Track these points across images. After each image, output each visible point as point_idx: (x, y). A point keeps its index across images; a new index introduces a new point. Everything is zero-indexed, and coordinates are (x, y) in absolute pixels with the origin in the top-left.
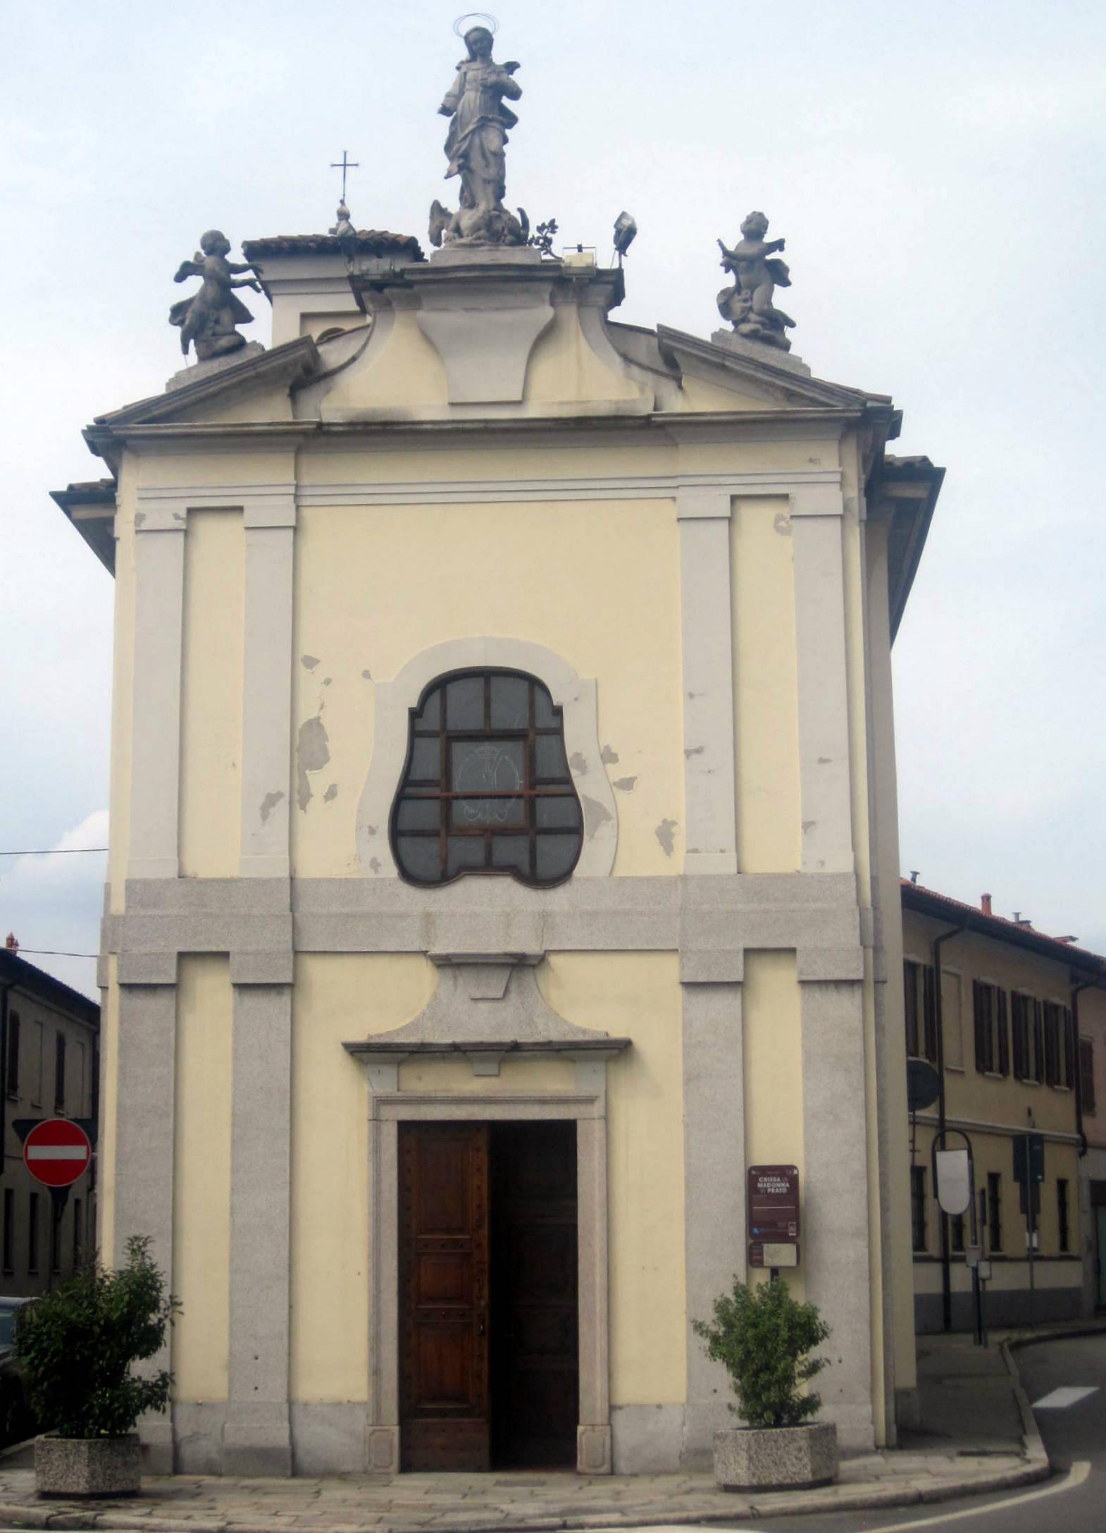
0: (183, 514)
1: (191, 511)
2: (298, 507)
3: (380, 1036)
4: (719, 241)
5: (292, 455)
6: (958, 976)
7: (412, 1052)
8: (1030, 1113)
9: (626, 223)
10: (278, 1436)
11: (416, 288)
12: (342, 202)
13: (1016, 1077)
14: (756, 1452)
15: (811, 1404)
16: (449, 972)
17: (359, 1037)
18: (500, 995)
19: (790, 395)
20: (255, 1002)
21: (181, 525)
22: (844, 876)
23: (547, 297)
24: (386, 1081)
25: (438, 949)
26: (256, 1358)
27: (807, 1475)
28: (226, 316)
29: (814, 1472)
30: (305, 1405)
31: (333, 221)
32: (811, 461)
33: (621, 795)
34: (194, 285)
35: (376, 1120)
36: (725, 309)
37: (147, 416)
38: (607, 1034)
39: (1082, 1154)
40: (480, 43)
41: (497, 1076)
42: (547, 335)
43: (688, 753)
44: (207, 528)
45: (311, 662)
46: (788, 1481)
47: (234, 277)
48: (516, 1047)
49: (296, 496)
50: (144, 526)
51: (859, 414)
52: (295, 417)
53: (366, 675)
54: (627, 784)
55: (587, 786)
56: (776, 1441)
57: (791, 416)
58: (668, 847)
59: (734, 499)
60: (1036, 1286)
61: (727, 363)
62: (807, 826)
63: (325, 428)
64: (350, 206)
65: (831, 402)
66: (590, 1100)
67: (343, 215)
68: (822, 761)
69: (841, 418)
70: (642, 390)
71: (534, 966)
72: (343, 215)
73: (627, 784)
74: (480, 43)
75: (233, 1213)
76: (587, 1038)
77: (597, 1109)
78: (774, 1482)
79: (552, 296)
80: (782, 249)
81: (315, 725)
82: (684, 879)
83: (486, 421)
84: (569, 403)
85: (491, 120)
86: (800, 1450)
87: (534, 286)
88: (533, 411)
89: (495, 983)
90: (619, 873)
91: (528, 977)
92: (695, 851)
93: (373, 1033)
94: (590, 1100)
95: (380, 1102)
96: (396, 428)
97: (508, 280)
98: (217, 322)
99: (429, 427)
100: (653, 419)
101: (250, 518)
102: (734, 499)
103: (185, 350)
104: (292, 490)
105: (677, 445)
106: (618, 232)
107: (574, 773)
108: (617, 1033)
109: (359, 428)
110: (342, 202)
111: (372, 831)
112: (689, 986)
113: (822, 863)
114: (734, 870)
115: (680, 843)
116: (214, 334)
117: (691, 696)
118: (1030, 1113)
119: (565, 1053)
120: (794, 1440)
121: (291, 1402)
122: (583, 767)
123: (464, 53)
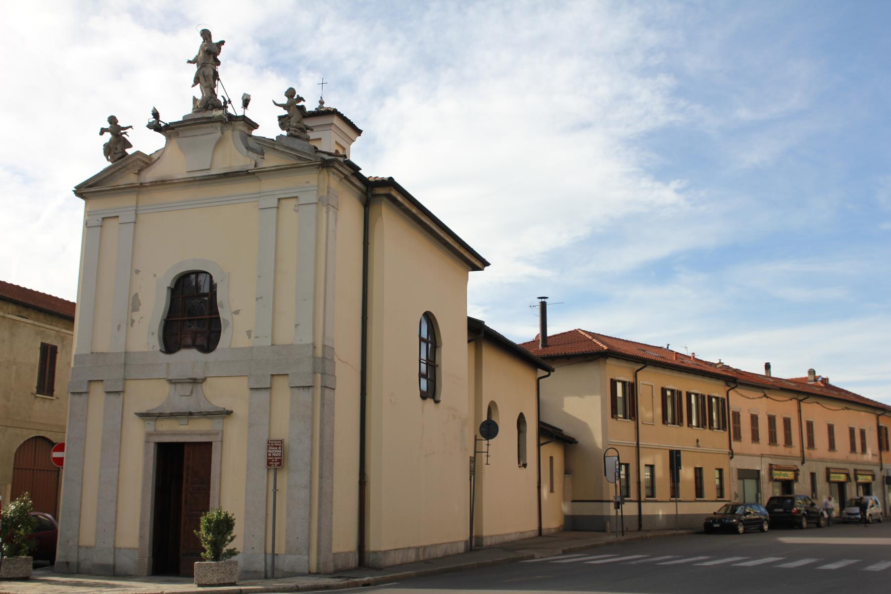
0: (100, 219)
1: (103, 219)
2: (136, 215)
3: (153, 410)
4: (273, 101)
5: (136, 196)
6: (652, 386)
7: (158, 416)
8: (698, 441)
9: (245, 97)
10: (109, 560)
11: (176, 129)
12: (321, 97)
13: (710, 428)
14: (198, 571)
15: (232, 553)
16: (173, 386)
17: (143, 410)
18: (189, 394)
19: (299, 158)
20: (112, 396)
21: (99, 223)
22: (308, 345)
23: (219, 128)
24: (151, 426)
25: (172, 376)
26: (104, 531)
27: (215, 582)
28: (119, 147)
29: (218, 581)
30: (120, 548)
31: (317, 105)
32: (307, 182)
33: (235, 316)
34: (108, 136)
35: (147, 442)
36: (282, 126)
37: (88, 185)
38: (224, 409)
39: (731, 458)
40: (206, 34)
41: (188, 425)
42: (219, 142)
43: (257, 299)
44: (111, 224)
45: (137, 272)
46: (208, 583)
47: (122, 131)
48: (191, 414)
49: (136, 210)
50: (88, 226)
51: (320, 163)
52: (138, 180)
53: (155, 275)
54: (237, 312)
55: (223, 314)
56: (205, 567)
57: (296, 166)
58: (250, 336)
59: (279, 199)
60: (679, 513)
61: (275, 147)
62: (296, 326)
63: (143, 185)
64: (324, 100)
65: (311, 159)
66: (217, 434)
67: (322, 102)
68: (305, 300)
69: (317, 164)
70: (251, 161)
71: (201, 383)
72: (322, 102)
73: (237, 312)
74: (206, 34)
75: (100, 476)
76: (215, 410)
77: (219, 438)
78: (204, 583)
79: (222, 129)
80: (304, 101)
81: (136, 295)
82: (252, 348)
83: (195, 177)
84: (225, 168)
85: (207, 64)
86: (213, 570)
87: (214, 124)
88: (214, 172)
89: (188, 388)
90: (233, 346)
91: (199, 386)
92: (257, 337)
93: (149, 409)
94: (217, 434)
95: (149, 435)
96: (165, 182)
97: (204, 123)
98: (116, 149)
99: (176, 181)
100: (249, 171)
101: (121, 220)
102: (279, 199)
103: (108, 160)
104: (134, 208)
105: (261, 181)
106: (244, 101)
107: (219, 308)
108: (228, 408)
109: (154, 184)
110: (321, 97)
111: (153, 334)
112: (251, 389)
113: (301, 340)
114: (270, 344)
115: (253, 334)
116: (115, 153)
117: (259, 277)
118: (698, 441)
119: (208, 416)
120: (211, 567)
121: (115, 548)
122: (222, 307)
123: (202, 40)
